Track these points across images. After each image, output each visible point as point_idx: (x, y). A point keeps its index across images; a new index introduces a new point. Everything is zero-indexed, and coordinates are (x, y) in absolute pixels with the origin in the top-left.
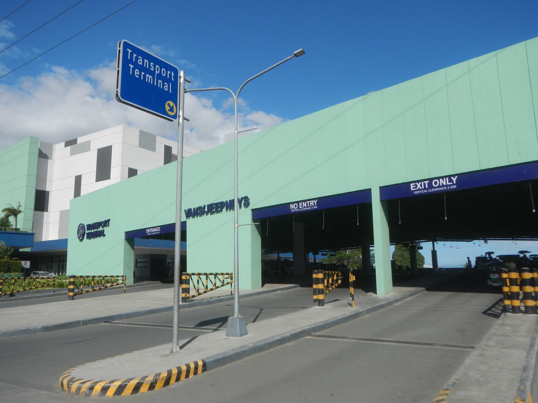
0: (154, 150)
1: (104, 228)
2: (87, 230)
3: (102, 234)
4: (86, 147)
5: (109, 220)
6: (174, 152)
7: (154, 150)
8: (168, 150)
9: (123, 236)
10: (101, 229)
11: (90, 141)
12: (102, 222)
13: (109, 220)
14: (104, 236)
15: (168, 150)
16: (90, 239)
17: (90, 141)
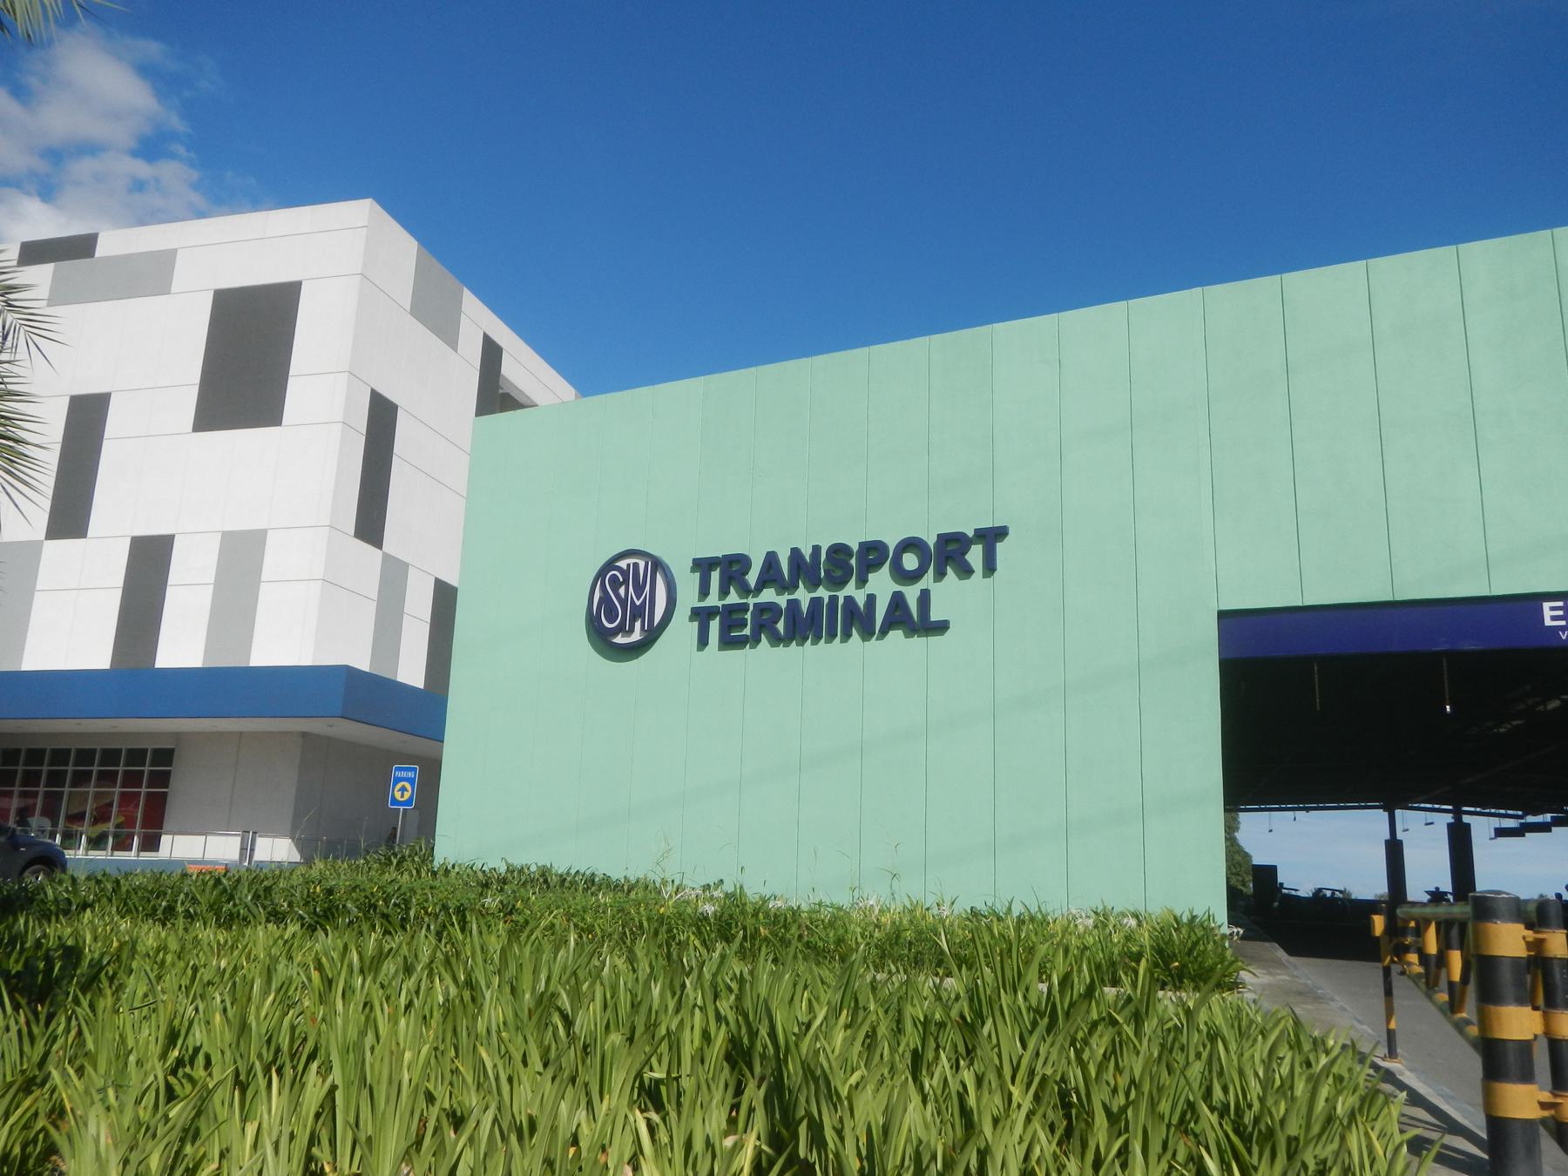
0: (453, 343)
1: (927, 581)
2: (704, 591)
3: (914, 621)
4: (151, 276)
5: (991, 537)
6: (508, 369)
7: (453, 343)
8: (492, 353)
9: (1209, 632)
10: (881, 584)
11: (175, 251)
12: (910, 544)
13: (991, 537)
14: (927, 626)
15: (492, 353)
16: (729, 642)
17: (175, 251)
